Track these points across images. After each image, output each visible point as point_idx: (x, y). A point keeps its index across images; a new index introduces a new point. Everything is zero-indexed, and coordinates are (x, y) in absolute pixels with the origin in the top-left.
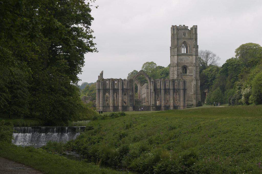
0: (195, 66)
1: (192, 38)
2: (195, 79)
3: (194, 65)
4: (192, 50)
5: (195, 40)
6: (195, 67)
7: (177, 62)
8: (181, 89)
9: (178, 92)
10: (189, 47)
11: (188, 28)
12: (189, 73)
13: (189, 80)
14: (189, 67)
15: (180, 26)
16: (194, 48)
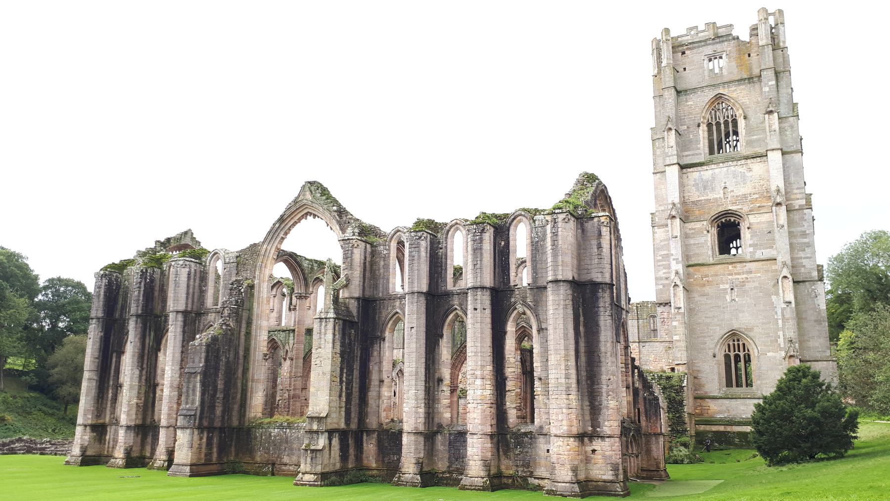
0: (779, 204)
1: (756, 72)
2: (785, 272)
3: (779, 200)
4: (764, 130)
5: (769, 75)
6: (784, 207)
7: (677, 194)
8: (550, 278)
9: (537, 316)
10: (745, 118)
11: (735, 33)
12: (750, 246)
13: (756, 284)
14: (752, 219)
15: (692, 33)
16: (771, 112)
